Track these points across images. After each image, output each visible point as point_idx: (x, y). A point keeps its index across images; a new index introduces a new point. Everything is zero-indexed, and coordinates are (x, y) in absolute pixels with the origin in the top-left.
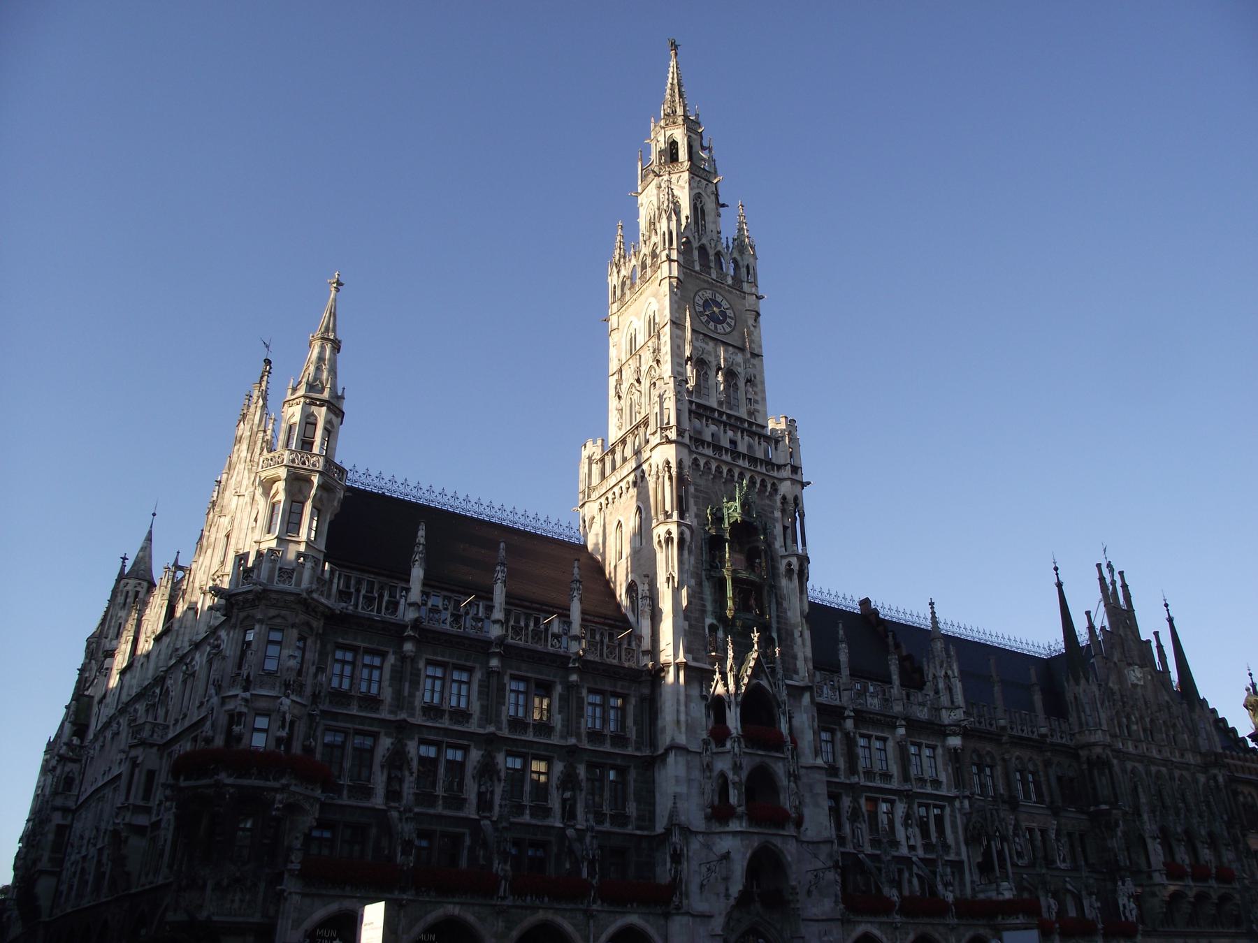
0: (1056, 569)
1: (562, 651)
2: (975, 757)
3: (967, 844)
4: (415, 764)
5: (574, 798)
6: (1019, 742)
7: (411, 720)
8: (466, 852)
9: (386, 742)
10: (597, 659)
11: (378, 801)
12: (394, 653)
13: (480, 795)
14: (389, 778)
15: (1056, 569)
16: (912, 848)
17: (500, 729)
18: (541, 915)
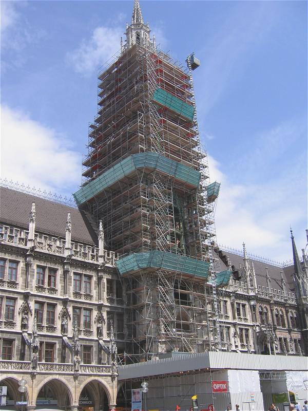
0: (291, 231)
1: (95, 263)
2: (260, 309)
3: (258, 345)
4: (33, 312)
5: (102, 327)
6: (277, 303)
7: (32, 293)
8: (57, 351)
9: (20, 303)
10: (111, 266)
11: (18, 329)
12: (23, 262)
13: (62, 326)
14: (23, 319)
15: (291, 231)
16: (236, 346)
17: (70, 297)
18: (93, 378)
